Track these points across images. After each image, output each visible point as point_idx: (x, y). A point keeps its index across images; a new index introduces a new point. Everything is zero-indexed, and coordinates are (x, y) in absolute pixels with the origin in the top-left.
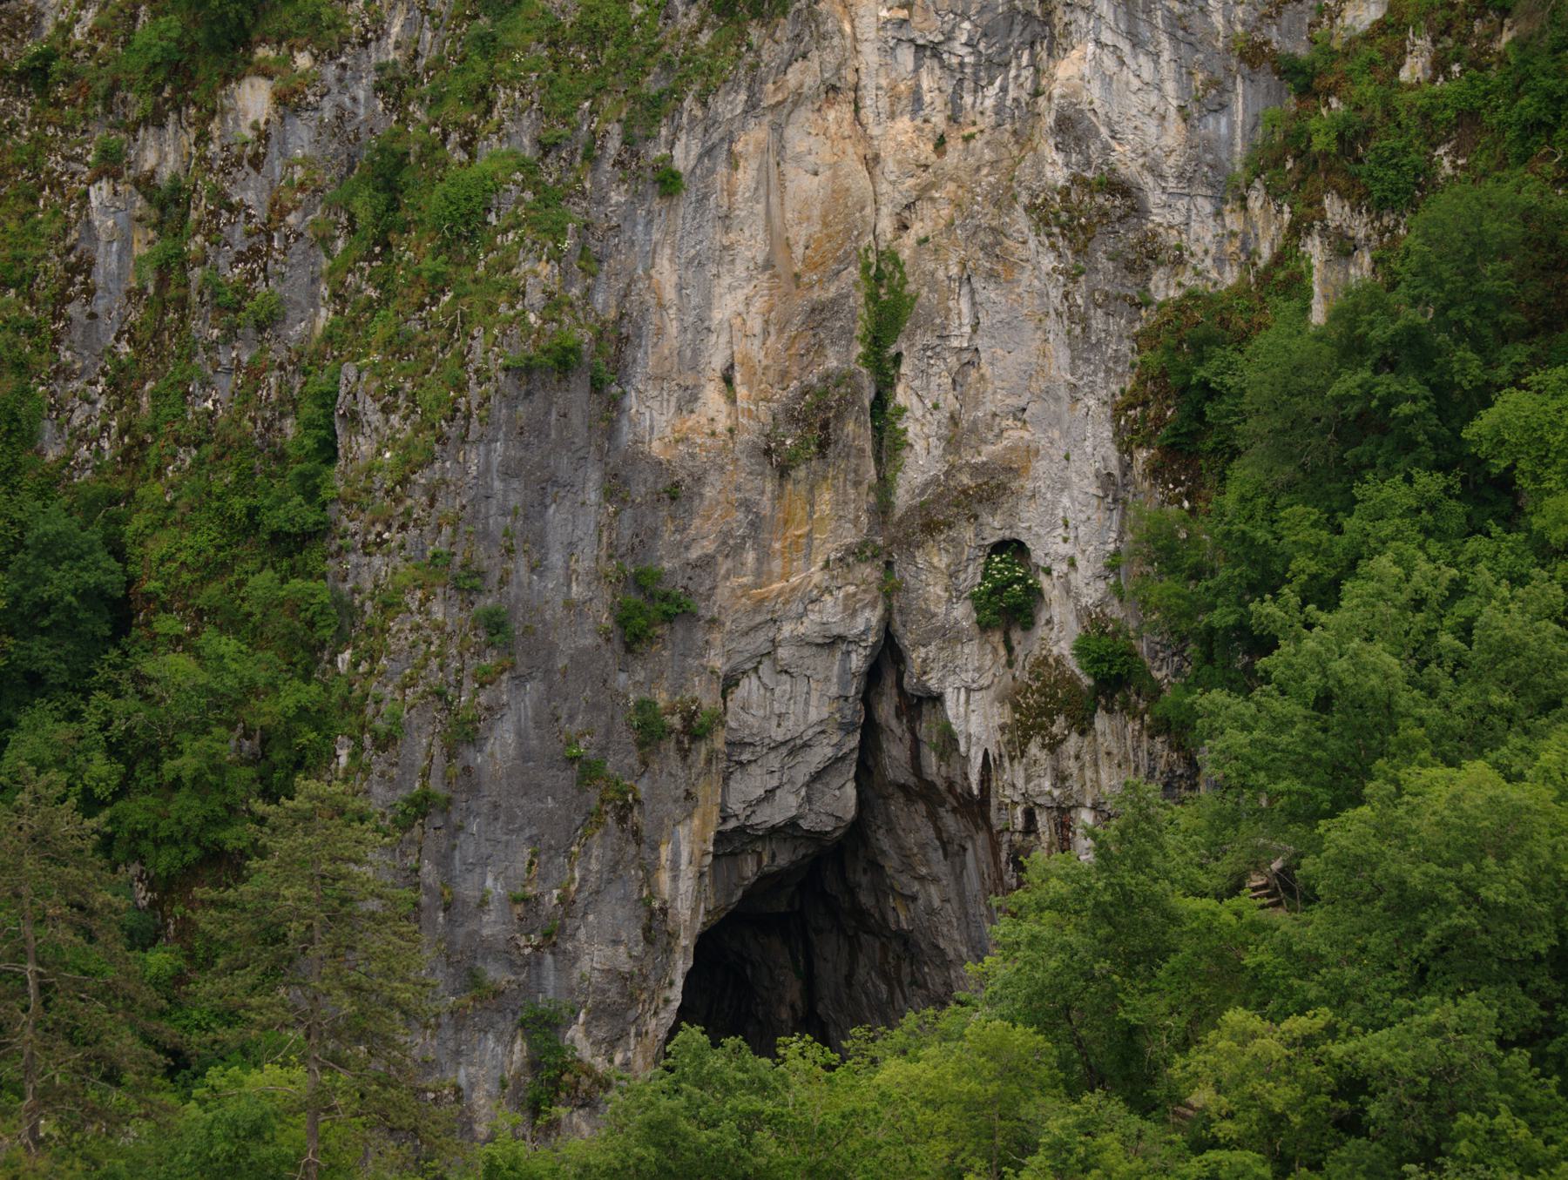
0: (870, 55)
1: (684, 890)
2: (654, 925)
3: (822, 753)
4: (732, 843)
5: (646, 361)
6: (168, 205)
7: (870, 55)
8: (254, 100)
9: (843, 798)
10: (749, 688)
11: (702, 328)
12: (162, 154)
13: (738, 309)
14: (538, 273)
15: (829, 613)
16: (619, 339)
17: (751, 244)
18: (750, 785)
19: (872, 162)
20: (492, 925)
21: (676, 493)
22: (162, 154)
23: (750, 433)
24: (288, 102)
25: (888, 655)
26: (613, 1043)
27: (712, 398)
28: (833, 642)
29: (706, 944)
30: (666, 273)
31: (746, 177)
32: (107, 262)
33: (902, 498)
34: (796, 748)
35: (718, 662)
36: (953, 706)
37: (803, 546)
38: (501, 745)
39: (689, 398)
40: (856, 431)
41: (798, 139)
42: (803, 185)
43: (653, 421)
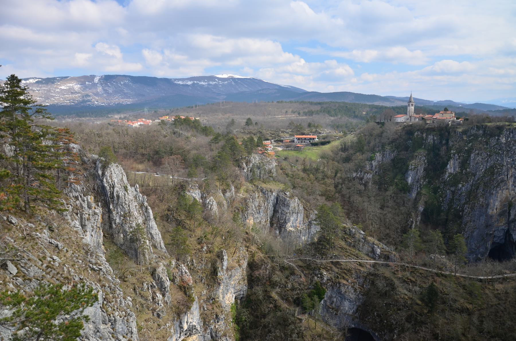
0: (510, 186)
1: (489, 245)
2: (486, 248)
3: (502, 237)
4: (493, 243)
5: (490, 207)
6: (453, 193)
7: (510, 186)
8: (460, 186)
9: (503, 241)
10: (496, 232)
11: (495, 205)
12: (452, 189)
13: (497, 204)
14: (481, 200)
15: (503, 227)
16: (488, 205)
17: (499, 199)
18: (495, 239)
19: (510, 194)
20: (473, 247)
21: (491, 217)
22: (452, 189)
23: (498, 213)
24: (463, 186)
25: (508, 231)
26: (482, 256)
27: (495, 210)
28: (503, 229)
29: (491, 250)
30: (492, 201)
31: (499, 195)
32: (448, 196)
33: (510, 219)
34: (499, 237)
35: (493, 230)
36: (513, 235)
37: (502, 222)
38: (475, 233)
39: (493, 210)
40: (507, 214)
41: (504, 192)
42: (504, 195)
43: (490, 212)
